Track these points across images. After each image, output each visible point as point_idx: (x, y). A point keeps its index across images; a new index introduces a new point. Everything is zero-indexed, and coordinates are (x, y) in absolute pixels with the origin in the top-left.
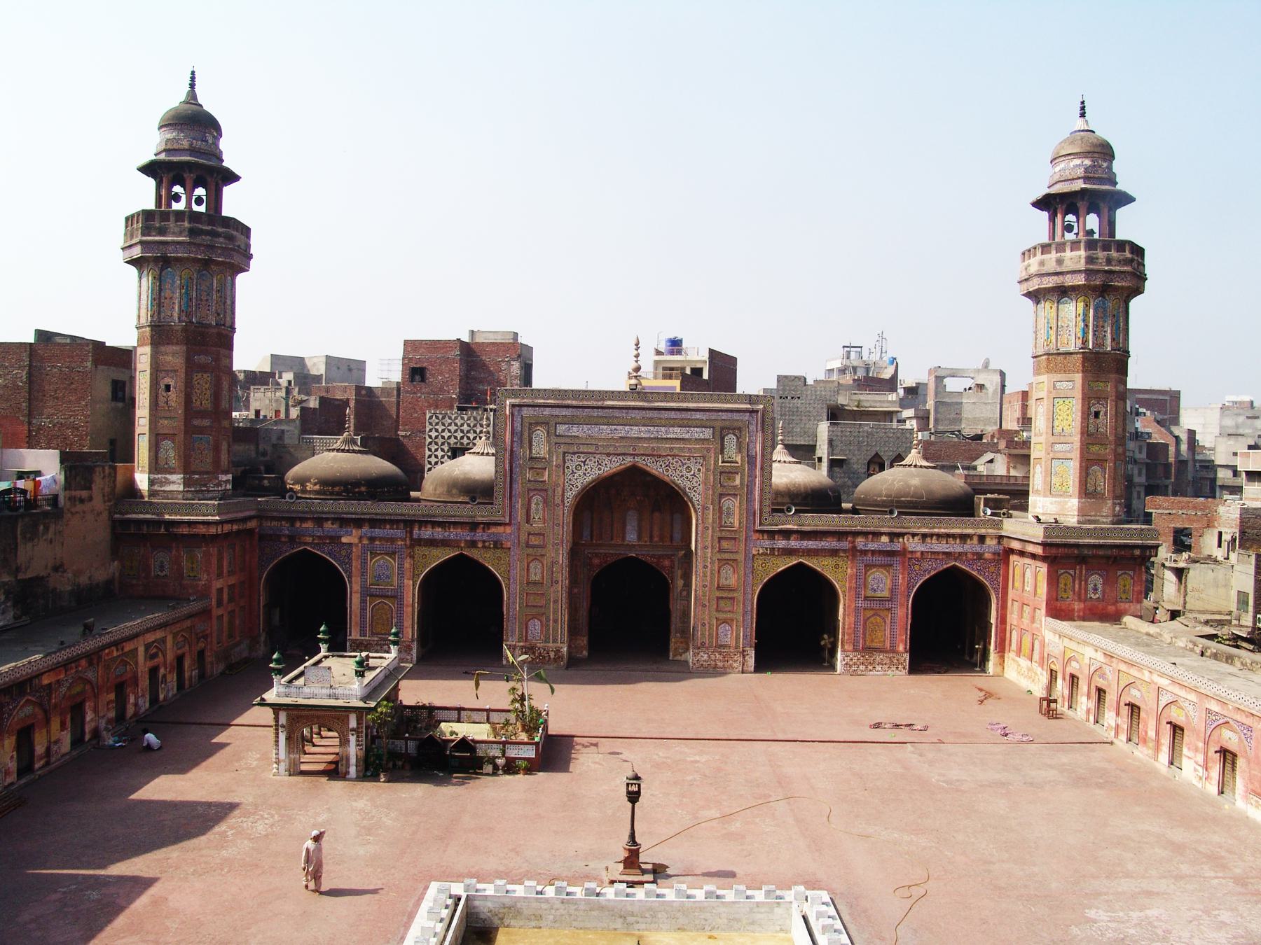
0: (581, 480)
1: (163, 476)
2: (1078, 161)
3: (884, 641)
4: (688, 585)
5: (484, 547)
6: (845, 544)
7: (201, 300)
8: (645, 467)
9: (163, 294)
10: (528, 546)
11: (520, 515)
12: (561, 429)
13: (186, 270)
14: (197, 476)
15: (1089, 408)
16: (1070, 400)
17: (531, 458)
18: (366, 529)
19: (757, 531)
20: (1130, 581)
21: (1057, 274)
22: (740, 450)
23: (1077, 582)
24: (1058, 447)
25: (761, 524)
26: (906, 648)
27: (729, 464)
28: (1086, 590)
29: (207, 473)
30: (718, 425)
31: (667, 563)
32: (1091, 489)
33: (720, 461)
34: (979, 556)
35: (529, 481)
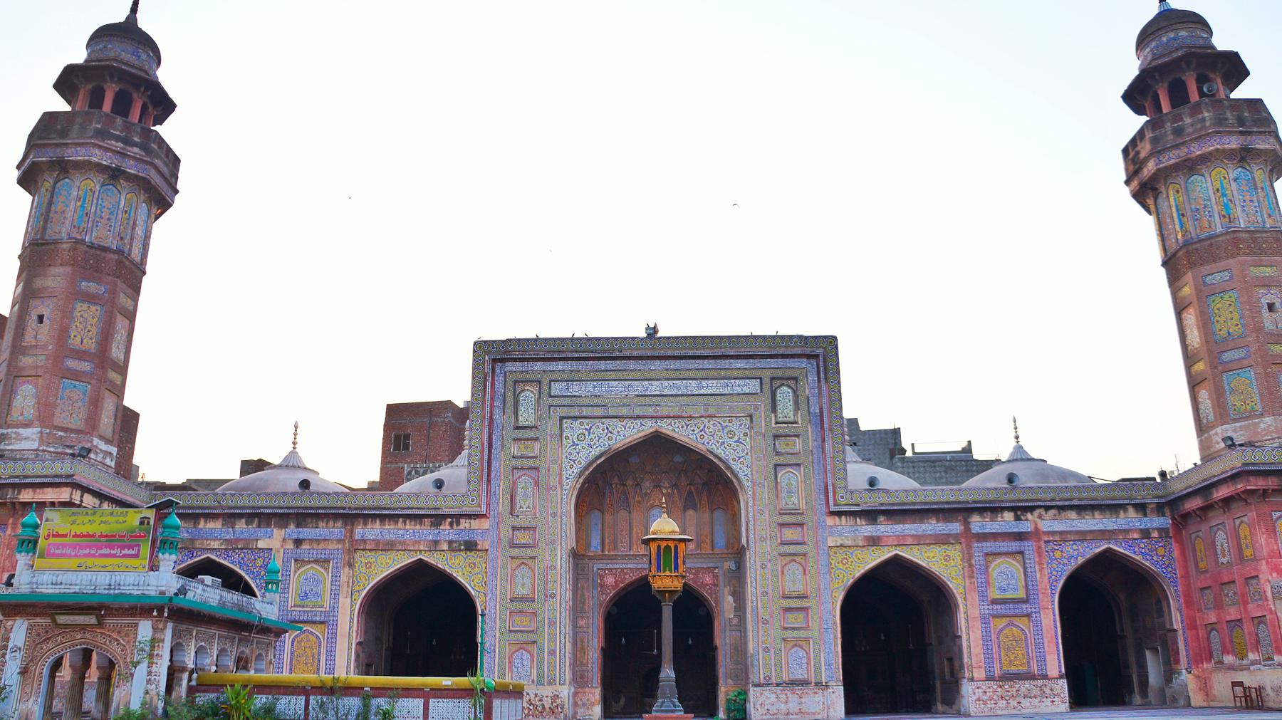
0: (584, 454)
1: (14, 430)
2: (1172, 35)
3: (1029, 662)
5: (450, 550)
6: (956, 527)
7: (102, 218)
8: (668, 433)
9: (53, 208)
11: (502, 504)
12: (557, 388)
13: (89, 181)
14: (60, 433)
17: (518, 428)
18: (292, 531)
21: (1176, 146)
24: (1227, 356)
25: (835, 505)
26: (1060, 672)
29: (78, 432)
30: (767, 375)
31: (708, 579)
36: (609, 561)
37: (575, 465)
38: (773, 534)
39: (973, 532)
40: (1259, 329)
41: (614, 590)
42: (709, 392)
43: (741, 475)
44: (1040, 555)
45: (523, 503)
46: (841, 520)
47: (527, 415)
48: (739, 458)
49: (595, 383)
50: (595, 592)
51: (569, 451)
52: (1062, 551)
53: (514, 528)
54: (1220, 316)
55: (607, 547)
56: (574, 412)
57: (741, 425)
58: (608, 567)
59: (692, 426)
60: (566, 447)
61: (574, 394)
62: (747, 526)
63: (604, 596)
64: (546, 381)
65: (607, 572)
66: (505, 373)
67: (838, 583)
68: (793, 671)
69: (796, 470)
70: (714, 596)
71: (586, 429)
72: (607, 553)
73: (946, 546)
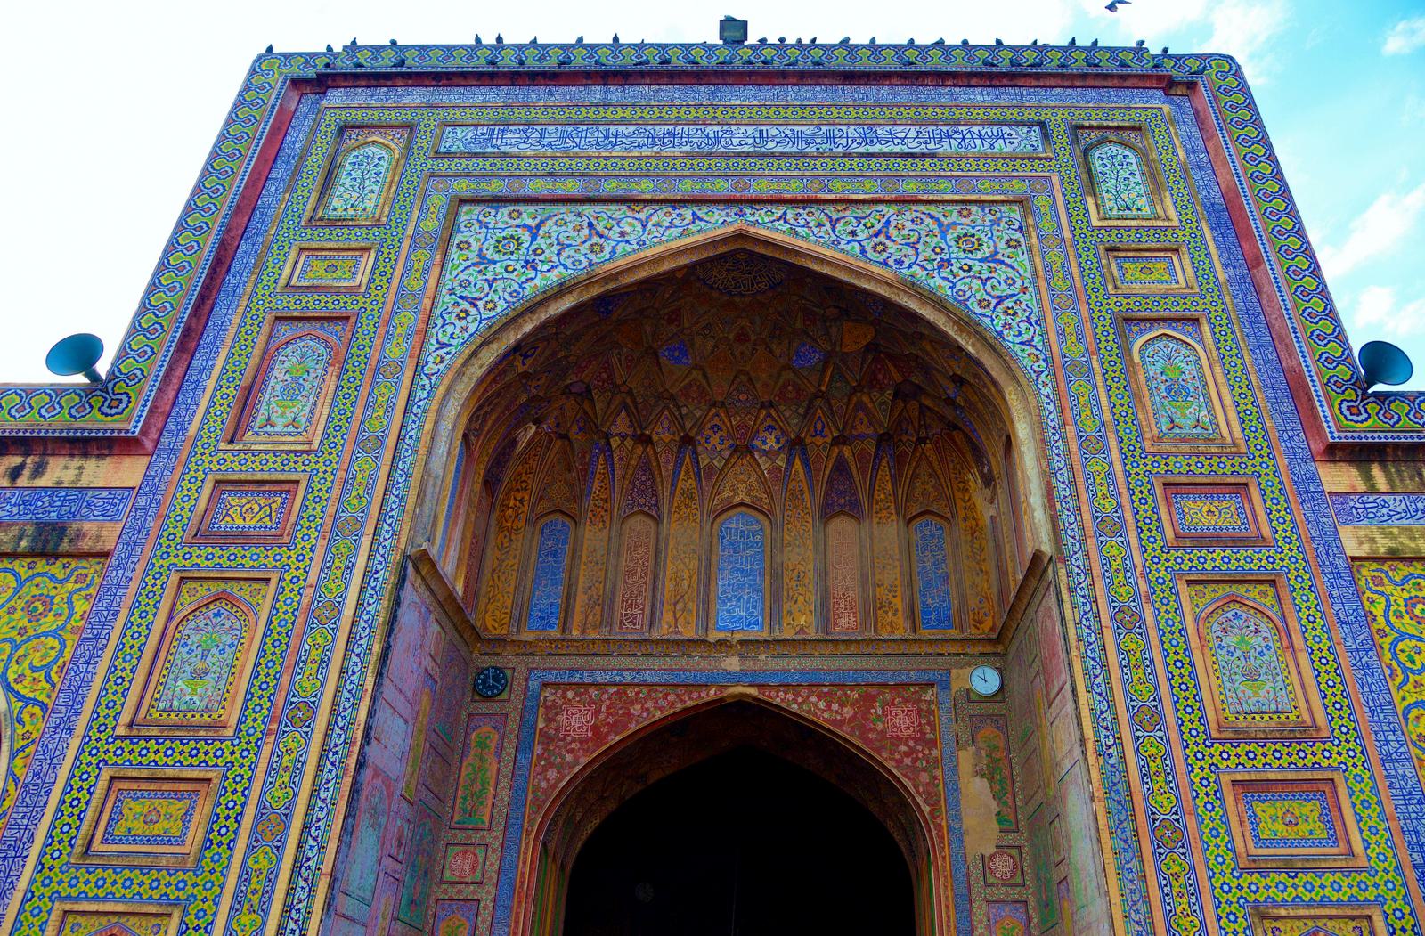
12: (457, 140)
31: (902, 722)
36: (581, 661)
41: (587, 751)
48: (1000, 300)
51: (463, 276)
55: (577, 618)
56: (495, 187)
57: (996, 222)
58: (577, 678)
61: (503, 149)
63: (552, 774)
65: (570, 694)
70: (925, 777)
71: (525, 226)
72: (575, 633)
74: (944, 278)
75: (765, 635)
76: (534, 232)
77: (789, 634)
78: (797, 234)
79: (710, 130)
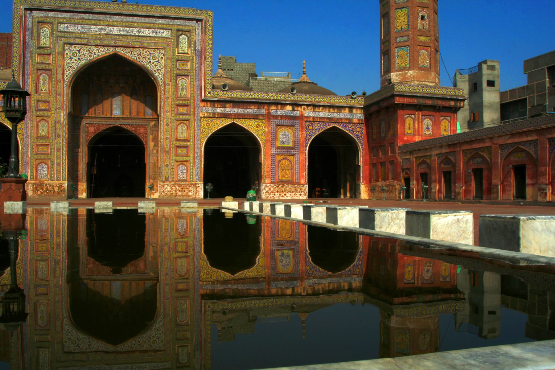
4: (156, 146)
6: (263, 111)
8: (123, 55)
10: (37, 110)
12: (62, 27)
15: (418, 13)
16: (406, 9)
19: (203, 101)
20: (447, 124)
22: (189, 46)
23: (416, 123)
25: (205, 96)
26: (305, 181)
27: (183, 55)
28: (422, 129)
30: (175, 28)
31: (142, 130)
32: (421, 65)
33: (176, 53)
34: (350, 121)
35: (38, 63)
37: (71, 69)
38: (173, 109)
39: (272, 114)
40: (415, 27)
42: (144, 35)
43: (158, 78)
44: (302, 128)
45: (43, 88)
46: (207, 104)
47: (45, 41)
49: (83, 26)
50: (84, 135)
51: (68, 61)
52: (313, 126)
53: (38, 101)
54: (399, 19)
56: (71, 41)
57: (160, 53)
58: (91, 123)
59: (134, 52)
60: (66, 59)
61: (71, 31)
62: (160, 105)
63: (89, 137)
64: (55, 23)
66: (33, 17)
67: (204, 135)
68: (180, 176)
69: (186, 78)
70: (145, 139)
71: (77, 50)
73: (258, 120)
74: (149, 65)
75: (121, 116)
76: (79, 51)
77: (125, 117)
78: (125, 54)
79: (110, 28)
